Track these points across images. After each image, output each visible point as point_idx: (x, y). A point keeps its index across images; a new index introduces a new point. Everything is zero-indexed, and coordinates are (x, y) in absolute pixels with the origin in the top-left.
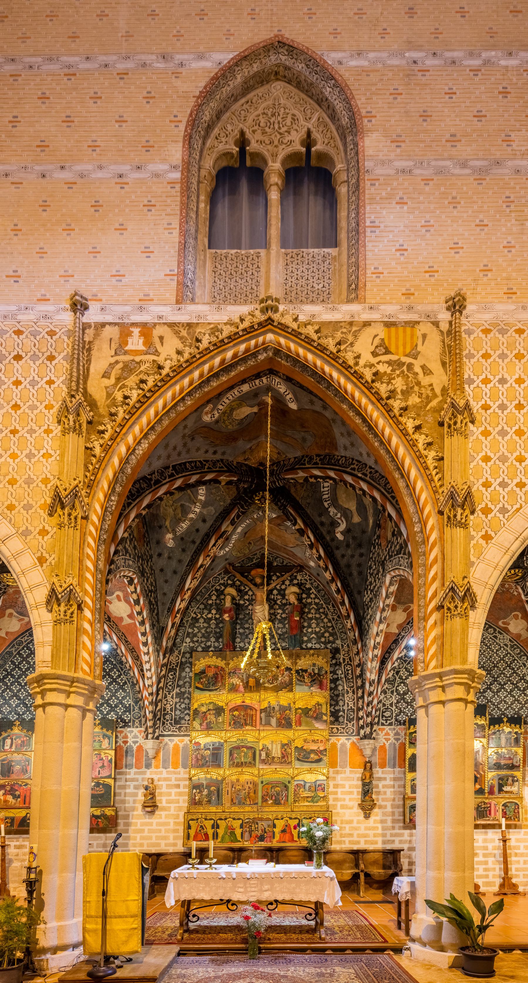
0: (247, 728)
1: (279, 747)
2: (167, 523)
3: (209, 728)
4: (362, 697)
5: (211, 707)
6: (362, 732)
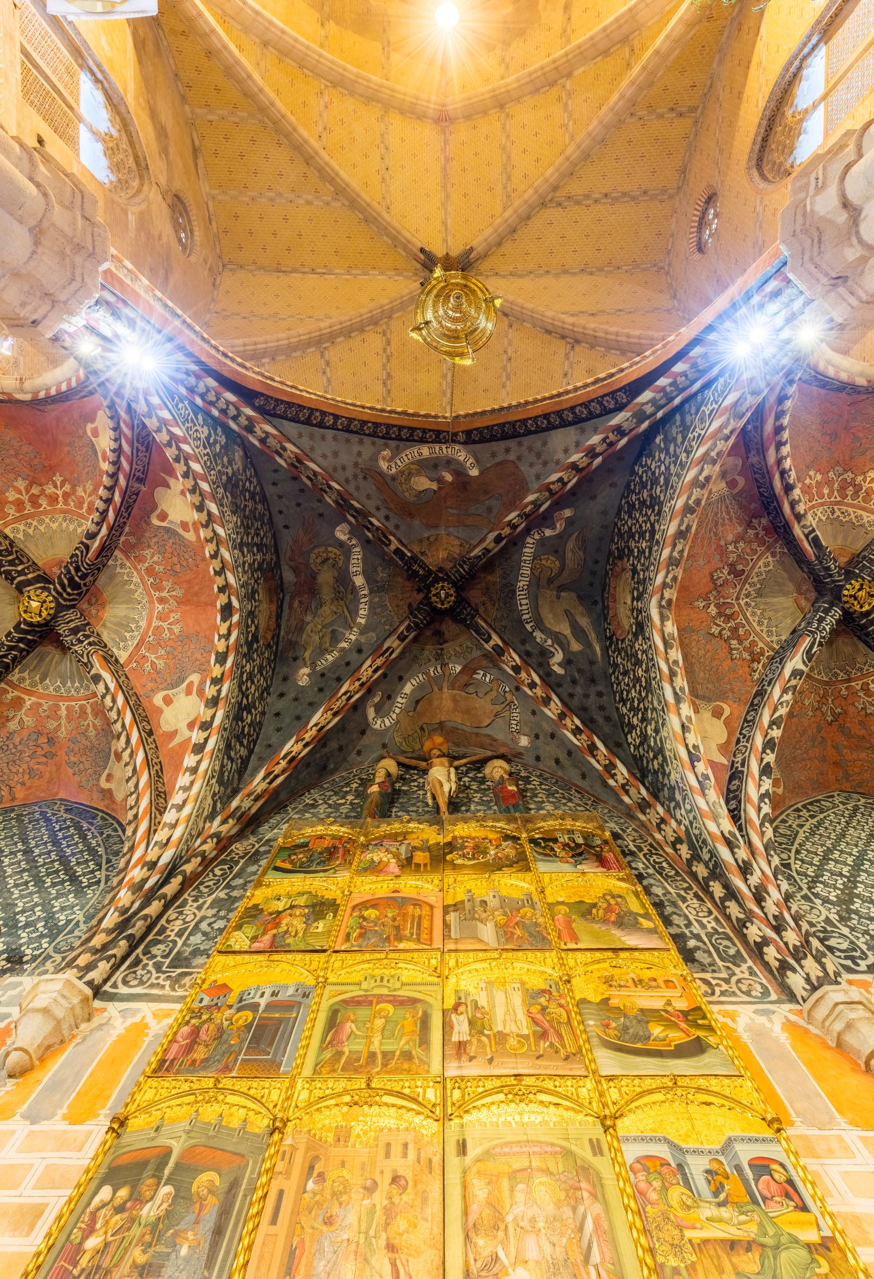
0: (401, 946)
1: (517, 999)
2: (307, 655)
3: (276, 948)
4: (731, 893)
5: (301, 901)
6: (796, 981)
